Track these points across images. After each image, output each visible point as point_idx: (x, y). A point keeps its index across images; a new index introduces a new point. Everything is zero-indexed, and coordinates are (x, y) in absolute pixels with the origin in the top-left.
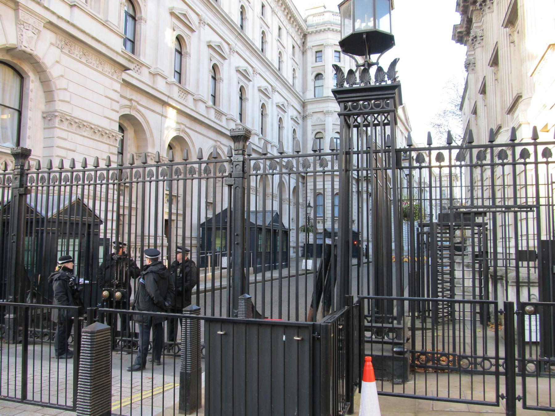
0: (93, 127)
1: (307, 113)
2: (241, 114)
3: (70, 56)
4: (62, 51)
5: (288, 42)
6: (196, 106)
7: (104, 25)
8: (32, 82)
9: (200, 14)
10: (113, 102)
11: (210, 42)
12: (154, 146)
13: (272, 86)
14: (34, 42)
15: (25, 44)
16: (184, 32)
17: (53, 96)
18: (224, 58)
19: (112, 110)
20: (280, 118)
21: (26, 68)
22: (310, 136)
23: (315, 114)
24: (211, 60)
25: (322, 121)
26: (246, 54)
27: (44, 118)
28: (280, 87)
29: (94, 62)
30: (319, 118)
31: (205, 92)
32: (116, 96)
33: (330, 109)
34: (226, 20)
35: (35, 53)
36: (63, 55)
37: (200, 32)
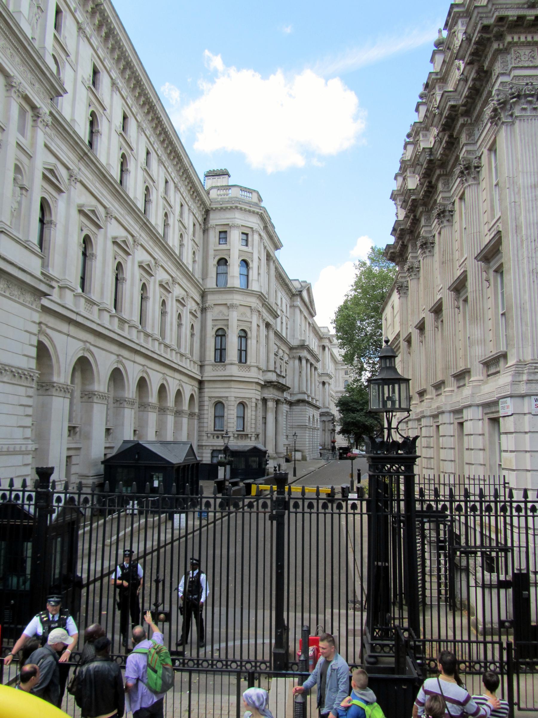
9: (71, 168)
12: (59, 374)
16: (91, 231)
20: (180, 314)
22: (210, 333)
23: (217, 307)
25: (225, 316)
26: (149, 244)
28: (181, 277)
30: (221, 312)
33: (235, 302)
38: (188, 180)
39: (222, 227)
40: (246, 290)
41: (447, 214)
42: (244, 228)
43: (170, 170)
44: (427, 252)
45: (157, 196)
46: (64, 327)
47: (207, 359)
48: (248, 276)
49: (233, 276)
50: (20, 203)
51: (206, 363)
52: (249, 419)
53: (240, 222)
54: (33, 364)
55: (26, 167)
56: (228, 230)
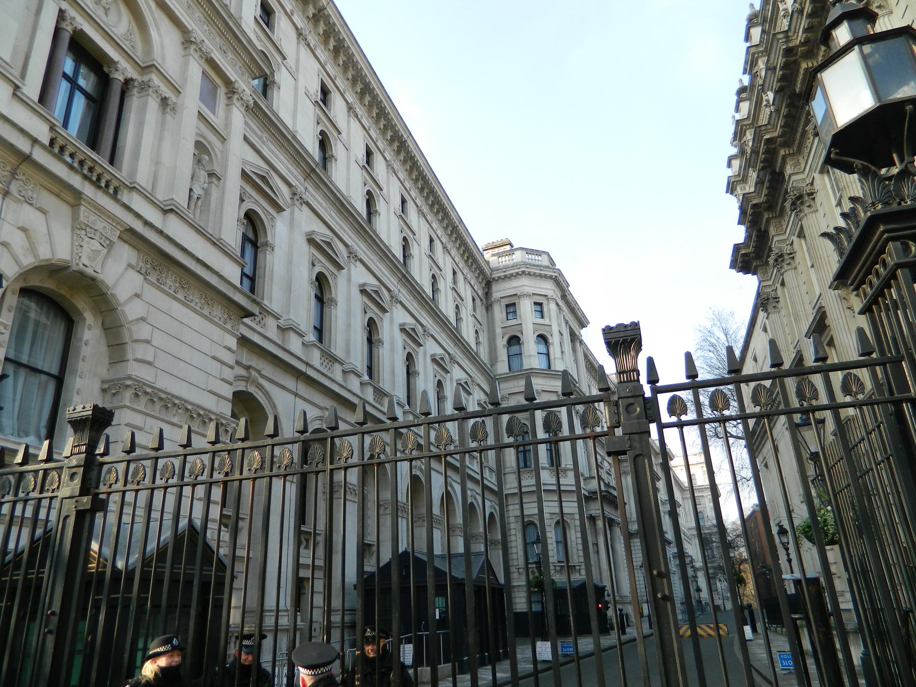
0: (189, 407)
2: (408, 397)
3: (158, 288)
4: (145, 279)
5: (466, 292)
6: (345, 380)
7: (215, 244)
8: (89, 329)
10: (224, 367)
11: (365, 284)
13: (449, 354)
14: (100, 259)
15: (85, 260)
17: (124, 351)
18: (384, 310)
19: (223, 380)
21: (81, 304)
23: (513, 397)
24: (366, 312)
27: (104, 391)
29: (197, 300)
31: (358, 360)
32: (229, 358)
34: (384, 253)
35: (101, 277)
36: (147, 286)
37: (349, 270)
38: (459, 242)
43: (434, 225)
45: (420, 252)
46: (290, 383)
47: (508, 464)
48: (548, 355)
50: (207, 192)
51: (507, 470)
52: (574, 545)
53: (531, 290)
54: (226, 409)
55: (217, 151)
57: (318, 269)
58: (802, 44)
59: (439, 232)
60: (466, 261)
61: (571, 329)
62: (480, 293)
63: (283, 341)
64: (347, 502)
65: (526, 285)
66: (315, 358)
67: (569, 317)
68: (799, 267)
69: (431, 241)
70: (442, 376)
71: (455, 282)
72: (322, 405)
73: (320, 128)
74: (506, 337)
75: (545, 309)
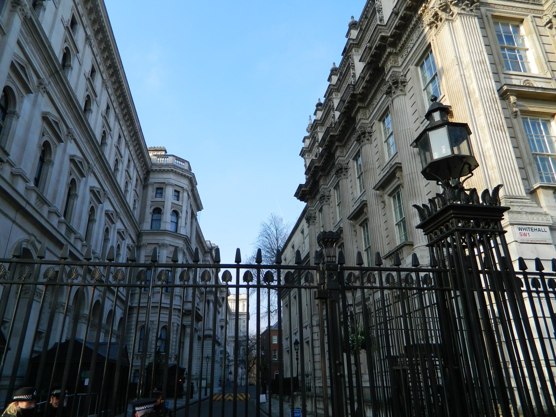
1: (142, 244)
5: (134, 174)
6: (49, 217)
18: (83, 175)
31: (59, 204)
33: (166, 242)
37: (66, 145)
39: (159, 185)
40: (175, 234)
41: (367, 135)
42: (177, 187)
43: (123, 128)
44: (342, 176)
48: (177, 223)
49: (166, 222)
53: (174, 182)
56: (164, 187)
57: (46, 138)
58: (360, 94)
59: (125, 133)
60: (138, 155)
61: (192, 210)
62: (141, 177)
63: (12, 182)
64: (117, 307)
65: (172, 178)
66: (33, 198)
67: (193, 203)
68: (331, 204)
69: (120, 137)
70: (109, 225)
71: (128, 166)
72: (31, 232)
73: (66, 45)
74: (153, 208)
75: (181, 196)
